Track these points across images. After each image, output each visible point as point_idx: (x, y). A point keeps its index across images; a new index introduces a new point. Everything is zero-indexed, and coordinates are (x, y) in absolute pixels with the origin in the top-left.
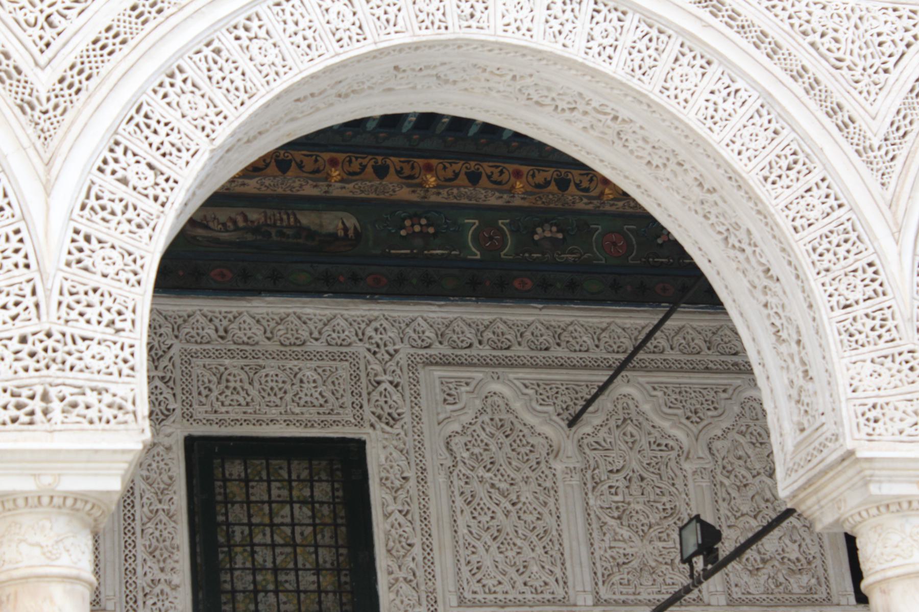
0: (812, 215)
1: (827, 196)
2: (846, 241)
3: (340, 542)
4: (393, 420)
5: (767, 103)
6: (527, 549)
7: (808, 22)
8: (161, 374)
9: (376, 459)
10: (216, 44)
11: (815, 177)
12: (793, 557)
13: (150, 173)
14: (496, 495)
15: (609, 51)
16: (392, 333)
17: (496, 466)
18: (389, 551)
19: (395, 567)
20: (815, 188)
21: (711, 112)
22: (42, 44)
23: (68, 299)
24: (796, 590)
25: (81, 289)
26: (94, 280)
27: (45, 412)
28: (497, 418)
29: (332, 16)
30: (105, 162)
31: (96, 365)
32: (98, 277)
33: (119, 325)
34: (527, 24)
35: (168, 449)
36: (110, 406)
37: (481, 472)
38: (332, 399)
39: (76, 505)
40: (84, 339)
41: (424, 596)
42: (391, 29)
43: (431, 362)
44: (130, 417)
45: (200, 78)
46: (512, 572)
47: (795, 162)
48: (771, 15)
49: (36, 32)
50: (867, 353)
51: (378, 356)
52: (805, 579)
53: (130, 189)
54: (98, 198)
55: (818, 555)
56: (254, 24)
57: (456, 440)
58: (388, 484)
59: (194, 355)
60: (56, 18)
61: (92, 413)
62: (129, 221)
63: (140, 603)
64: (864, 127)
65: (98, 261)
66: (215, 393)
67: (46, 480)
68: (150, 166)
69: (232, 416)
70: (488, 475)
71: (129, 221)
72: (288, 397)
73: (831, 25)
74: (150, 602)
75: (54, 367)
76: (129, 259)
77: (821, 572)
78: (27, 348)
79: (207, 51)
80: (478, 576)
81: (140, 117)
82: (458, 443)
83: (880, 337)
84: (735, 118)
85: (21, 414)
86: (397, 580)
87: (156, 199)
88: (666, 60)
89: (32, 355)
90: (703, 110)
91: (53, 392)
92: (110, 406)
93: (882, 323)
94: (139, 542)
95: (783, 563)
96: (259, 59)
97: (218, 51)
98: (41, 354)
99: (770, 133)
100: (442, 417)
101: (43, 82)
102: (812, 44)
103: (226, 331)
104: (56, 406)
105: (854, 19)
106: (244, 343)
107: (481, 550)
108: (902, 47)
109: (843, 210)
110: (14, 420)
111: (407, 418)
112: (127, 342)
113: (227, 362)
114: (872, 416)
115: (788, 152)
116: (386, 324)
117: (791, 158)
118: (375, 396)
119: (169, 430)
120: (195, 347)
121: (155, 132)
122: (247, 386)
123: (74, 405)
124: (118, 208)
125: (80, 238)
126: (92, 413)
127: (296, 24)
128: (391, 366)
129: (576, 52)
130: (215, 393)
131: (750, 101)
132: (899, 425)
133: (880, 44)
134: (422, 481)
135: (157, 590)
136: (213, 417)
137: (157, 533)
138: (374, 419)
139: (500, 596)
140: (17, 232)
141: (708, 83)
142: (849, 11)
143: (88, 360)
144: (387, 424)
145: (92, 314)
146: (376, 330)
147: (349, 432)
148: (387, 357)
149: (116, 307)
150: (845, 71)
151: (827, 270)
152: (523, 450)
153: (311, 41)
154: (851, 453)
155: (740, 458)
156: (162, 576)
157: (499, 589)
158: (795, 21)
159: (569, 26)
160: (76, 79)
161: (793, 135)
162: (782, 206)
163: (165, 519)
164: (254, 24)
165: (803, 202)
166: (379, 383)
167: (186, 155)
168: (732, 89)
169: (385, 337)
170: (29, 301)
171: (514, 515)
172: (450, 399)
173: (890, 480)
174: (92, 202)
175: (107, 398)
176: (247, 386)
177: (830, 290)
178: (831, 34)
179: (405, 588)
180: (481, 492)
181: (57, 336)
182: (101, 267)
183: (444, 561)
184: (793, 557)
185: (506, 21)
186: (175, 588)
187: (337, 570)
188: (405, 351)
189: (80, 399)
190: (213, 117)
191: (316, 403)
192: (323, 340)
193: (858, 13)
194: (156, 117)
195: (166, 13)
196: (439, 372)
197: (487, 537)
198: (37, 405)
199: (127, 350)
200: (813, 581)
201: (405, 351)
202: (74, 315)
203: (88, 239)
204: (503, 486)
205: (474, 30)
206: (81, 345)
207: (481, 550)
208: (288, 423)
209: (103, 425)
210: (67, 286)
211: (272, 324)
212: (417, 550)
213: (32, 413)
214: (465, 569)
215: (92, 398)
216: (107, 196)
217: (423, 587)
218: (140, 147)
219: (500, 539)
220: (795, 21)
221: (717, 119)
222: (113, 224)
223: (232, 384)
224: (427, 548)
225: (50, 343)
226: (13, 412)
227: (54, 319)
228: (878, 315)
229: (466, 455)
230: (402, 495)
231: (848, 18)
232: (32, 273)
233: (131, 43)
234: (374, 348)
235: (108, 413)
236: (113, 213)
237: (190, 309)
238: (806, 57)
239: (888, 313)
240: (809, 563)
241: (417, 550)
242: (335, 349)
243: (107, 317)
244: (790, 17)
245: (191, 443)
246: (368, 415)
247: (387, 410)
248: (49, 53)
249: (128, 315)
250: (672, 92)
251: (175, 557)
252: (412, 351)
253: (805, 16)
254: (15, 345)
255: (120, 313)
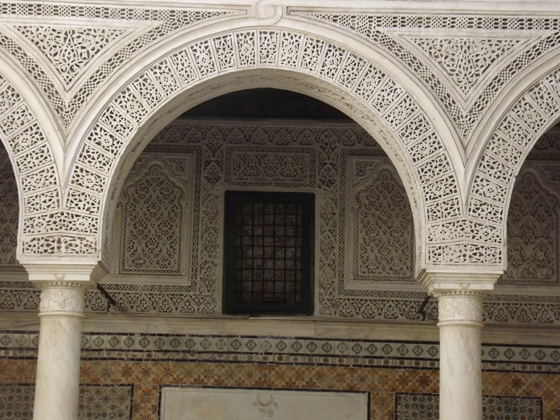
0: (424, 153)
1: (434, 142)
2: (440, 165)
3: (298, 246)
4: (331, 182)
5: (408, 98)
6: (393, 251)
7: (440, 51)
8: (216, 159)
9: (320, 203)
10: (145, 77)
11: (429, 133)
12: (541, 259)
13: (111, 140)
14: (380, 223)
15: (333, 71)
16: (334, 138)
17: (382, 208)
18: (322, 251)
19: (324, 259)
20: (428, 139)
21: (380, 101)
22: (68, 80)
23: (71, 198)
24: (539, 276)
25: (77, 193)
26: (83, 189)
27: (59, 248)
28: (385, 182)
29: (200, 60)
30: (92, 135)
31: (81, 228)
32: (85, 188)
33: (92, 210)
34: (294, 59)
35: (217, 197)
36: (86, 245)
37: (373, 211)
38: (300, 173)
39: (74, 284)
40: (77, 216)
41: (337, 273)
42: (227, 65)
43: (353, 154)
44: (93, 251)
45: (137, 93)
46: (384, 262)
47: (420, 125)
48: (420, 48)
49: (65, 74)
50: (440, 222)
51: (326, 150)
52: (545, 271)
53: (101, 148)
54: (88, 152)
55: (555, 258)
56: (163, 67)
57: (362, 194)
58: (325, 216)
59: (233, 149)
60: (75, 67)
61: (78, 249)
62: (100, 162)
63: (198, 272)
64: (460, 106)
65: (85, 181)
66: (242, 169)
67: (59, 276)
68: (111, 136)
69: (249, 181)
70: (377, 213)
71: (100, 162)
72: (278, 172)
73: (451, 52)
74: (203, 272)
75: (64, 228)
76: (98, 180)
77: (555, 267)
78: (53, 220)
79: (141, 80)
80: (366, 264)
81: (108, 113)
82: (363, 196)
83: (449, 213)
84: (392, 104)
85: (48, 248)
86: (324, 265)
87: (113, 151)
88: (362, 74)
89: (55, 223)
90: (376, 100)
91: (62, 239)
92: (86, 245)
93: (452, 206)
94: (200, 243)
95: (534, 262)
96: (164, 83)
97: (145, 80)
98: (58, 223)
99: (409, 111)
100: (355, 183)
101: (67, 98)
102: (440, 63)
103: (250, 137)
104: (63, 245)
105: (465, 48)
106: (259, 143)
107: (369, 251)
108: (488, 62)
109: (441, 149)
110: (46, 251)
111: (338, 183)
112: (95, 217)
113: (249, 153)
114: (436, 253)
115: (417, 120)
116: (331, 133)
117: (418, 124)
118: (322, 171)
119: (217, 188)
120: (233, 145)
121: (115, 120)
122: (258, 165)
123: (71, 245)
124: (96, 156)
125: (78, 170)
126: (78, 249)
127: (183, 65)
128: (332, 155)
129: (316, 73)
130: (242, 169)
131: (401, 94)
132: (450, 257)
133: (477, 61)
134: (342, 215)
135: (207, 266)
136: (239, 181)
137: (209, 239)
138: (320, 183)
139: (377, 275)
140: (52, 168)
141: (381, 86)
142: (463, 44)
143: (77, 225)
144: (327, 186)
145: (81, 205)
146: (326, 136)
147: (307, 190)
148: (331, 150)
149: (91, 202)
150: (455, 77)
151: (428, 180)
152: (397, 200)
153: (189, 73)
154: (424, 270)
155: (517, 205)
156: (210, 260)
157: (377, 271)
158: (433, 51)
159: (315, 59)
160: (79, 99)
161: (421, 112)
162: (409, 148)
163: (213, 232)
164: (163, 67)
165: (420, 146)
166: (325, 164)
167: (127, 131)
168: (393, 89)
169: (331, 140)
170: (55, 199)
171: (388, 234)
172: (361, 173)
173: (445, 282)
174: (85, 154)
175: (84, 242)
176: (258, 165)
177: (427, 190)
178: (451, 57)
179: (329, 269)
180: (373, 221)
181: (66, 215)
182: (86, 184)
183: (349, 256)
184: (541, 259)
185: (283, 58)
186: (215, 265)
187: (295, 259)
188: (340, 147)
189: (73, 242)
190: (141, 112)
191: (292, 174)
192: (298, 141)
193: (468, 44)
194: (115, 113)
195: (124, 62)
196: (355, 159)
197: (373, 244)
198: (55, 245)
199: (95, 221)
200: (550, 272)
201: (340, 147)
202: (73, 205)
203: (82, 170)
204: (384, 218)
205: (267, 64)
206: (76, 219)
207: (369, 251)
208: (277, 185)
209: (82, 254)
210: (71, 192)
211: (274, 133)
212: (336, 250)
213: (53, 248)
214: (360, 261)
215: (78, 242)
216: (91, 151)
217: (337, 269)
218: (107, 128)
219: (380, 246)
220: (433, 51)
221: (383, 104)
222: (93, 164)
223: (251, 165)
224: (342, 249)
225: (63, 218)
226: (46, 248)
227: (64, 207)
228: (450, 203)
229: (367, 202)
230: (331, 222)
231: (462, 47)
232: (57, 187)
233: (107, 78)
234: (324, 146)
235: (84, 249)
236: (94, 159)
237: (233, 126)
238: (434, 69)
239: (455, 202)
240: (549, 262)
241: (336, 250)
242: (304, 146)
243: (87, 206)
244: (431, 48)
245: (228, 195)
246: (318, 181)
247: (328, 178)
248: (71, 84)
249: (96, 205)
250: (361, 92)
251: (217, 250)
252: (343, 147)
253: (438, 47)
254: (47, 219)
255: (93, 204)
